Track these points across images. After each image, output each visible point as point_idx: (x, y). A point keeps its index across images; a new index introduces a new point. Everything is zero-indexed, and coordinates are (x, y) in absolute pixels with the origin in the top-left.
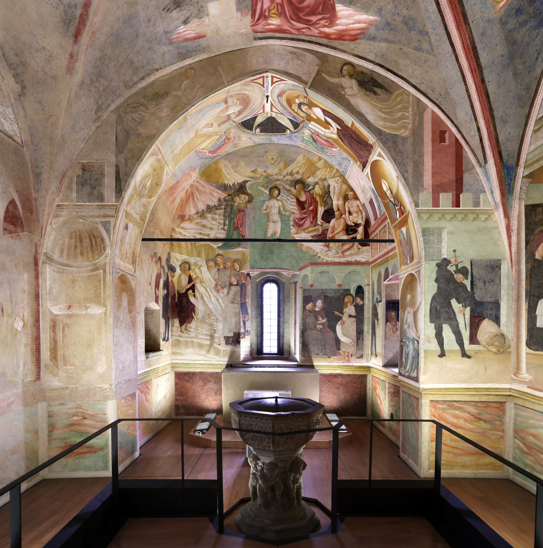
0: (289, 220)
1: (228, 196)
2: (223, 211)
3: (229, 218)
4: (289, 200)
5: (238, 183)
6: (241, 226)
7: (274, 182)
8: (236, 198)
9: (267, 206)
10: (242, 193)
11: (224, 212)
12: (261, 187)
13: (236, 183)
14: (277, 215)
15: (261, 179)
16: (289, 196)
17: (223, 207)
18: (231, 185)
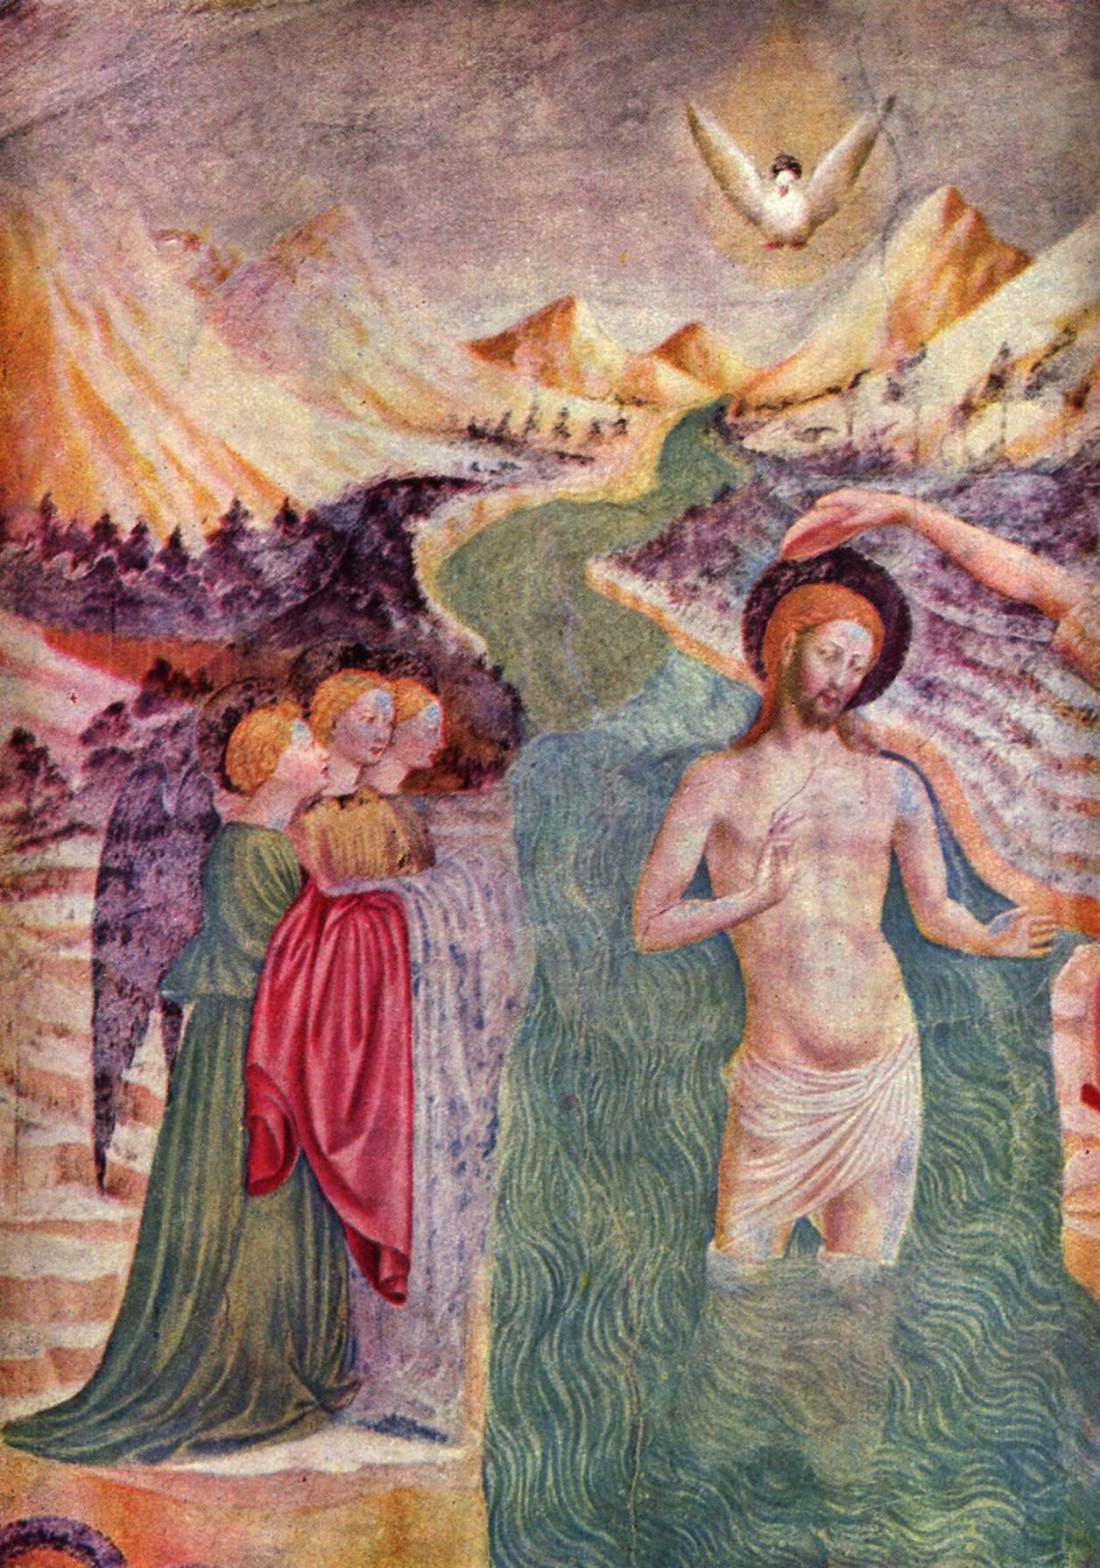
0: (1039, 1016)
1: (145, 705)
2: (80, 909)
3: (171, 1011)
4: (1028, 740)
5: (287, 517)
6: (348, 1124)
7: (810, 499)
8: (259, 726)
9: (723, 832)
10: (354, 659)
11: (100, 934)
12: (624, 562)
13: (261, 522)
14: (862, 946)
15: (623, 447)
16: (1026, 681)
17: (83, 854)
18: (196, 545)
